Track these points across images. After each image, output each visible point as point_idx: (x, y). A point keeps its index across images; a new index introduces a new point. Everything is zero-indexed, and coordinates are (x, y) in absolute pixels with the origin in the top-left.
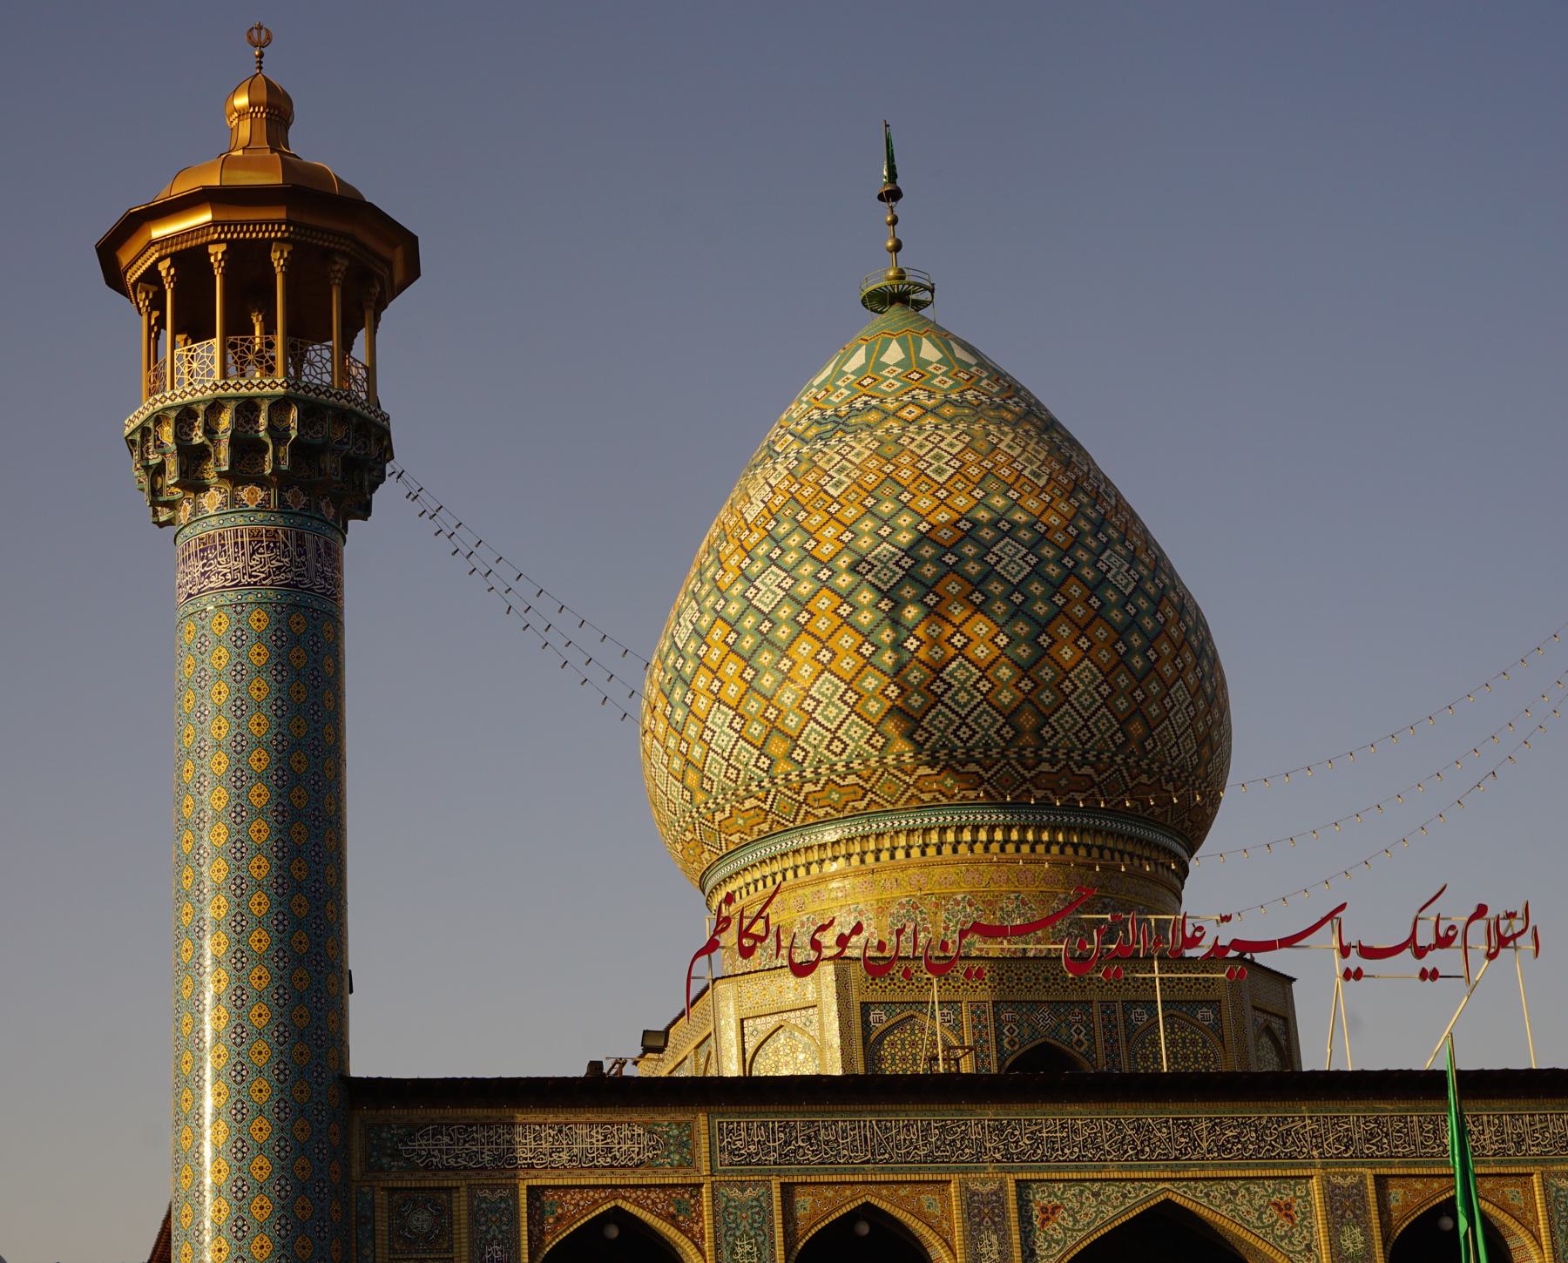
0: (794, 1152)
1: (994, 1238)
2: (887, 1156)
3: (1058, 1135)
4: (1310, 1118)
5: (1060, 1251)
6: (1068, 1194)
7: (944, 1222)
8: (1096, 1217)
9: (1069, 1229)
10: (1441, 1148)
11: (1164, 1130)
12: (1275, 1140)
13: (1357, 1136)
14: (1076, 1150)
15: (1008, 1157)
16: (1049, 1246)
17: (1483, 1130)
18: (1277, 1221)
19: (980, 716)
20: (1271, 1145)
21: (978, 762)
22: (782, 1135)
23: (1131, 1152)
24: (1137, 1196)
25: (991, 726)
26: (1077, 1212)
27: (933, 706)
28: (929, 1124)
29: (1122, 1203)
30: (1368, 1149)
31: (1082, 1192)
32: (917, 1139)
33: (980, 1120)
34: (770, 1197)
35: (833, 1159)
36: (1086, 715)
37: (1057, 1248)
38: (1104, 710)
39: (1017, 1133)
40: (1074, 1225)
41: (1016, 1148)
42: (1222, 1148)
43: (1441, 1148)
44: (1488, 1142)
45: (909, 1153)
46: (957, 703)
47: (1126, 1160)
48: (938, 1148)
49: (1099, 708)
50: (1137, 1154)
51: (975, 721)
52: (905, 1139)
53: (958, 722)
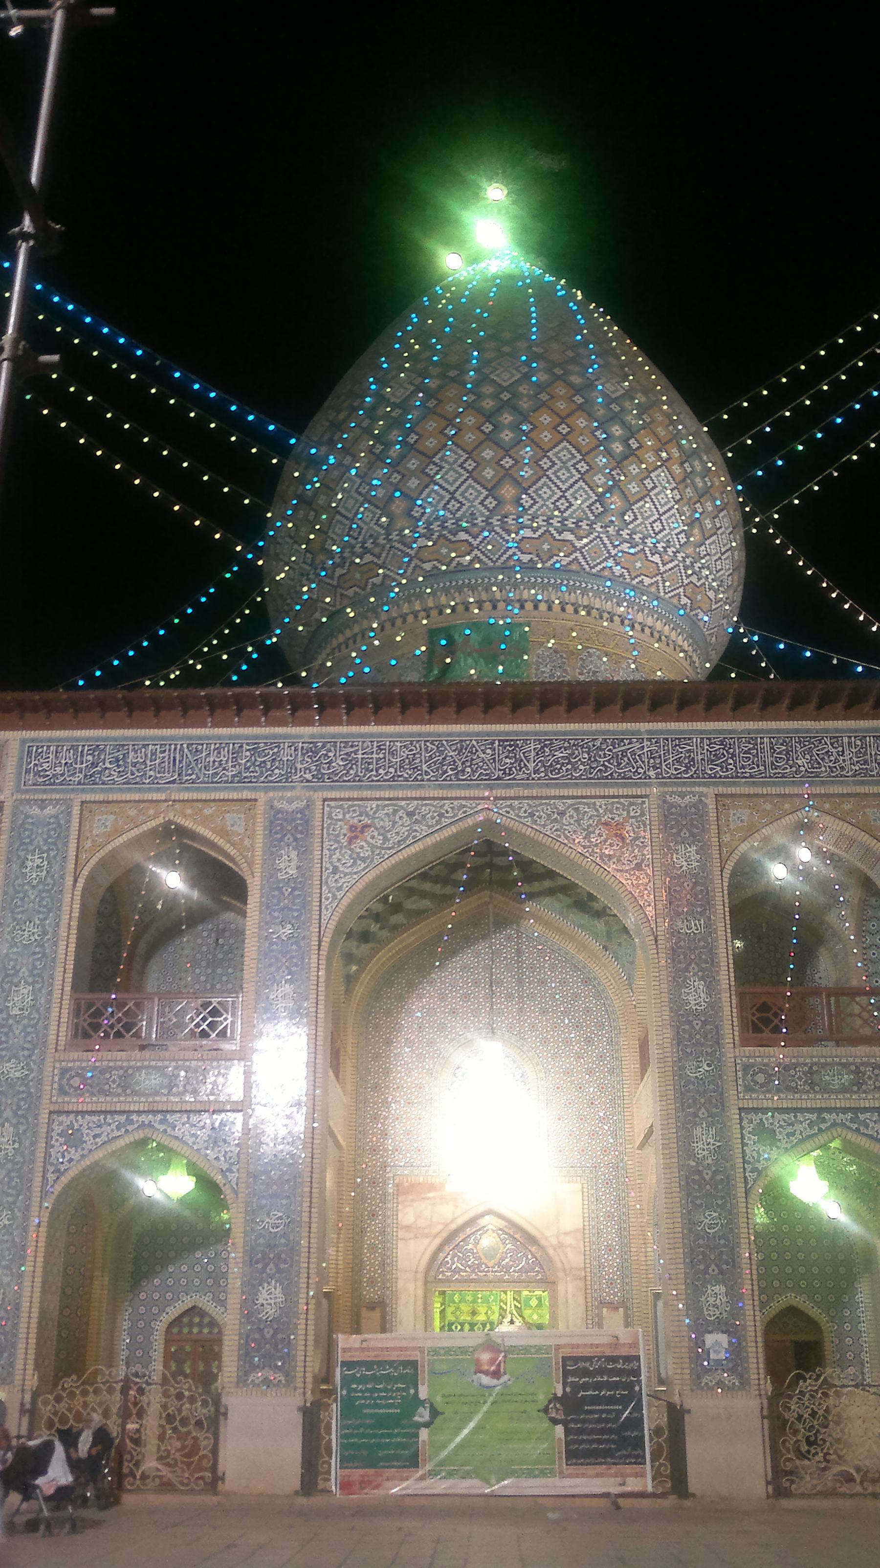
0: (100, 773)
1: (294, 854)
2: (194, 777)
3: (374, 756)
4: (650, 740)
5: (365, 868)
6: (381, 814)
7: (247, 840)
8: (408, 836)
9: (377, 847)
10: (794, 769)
11: (489, 751)
12: (608, 761)
13: (700, 757)
14: (392, 770)
15: (318, 776)
16: (354, 864)
17: (843, 752)
18: (605, 841)
19: (465, 491)
20: (603, 765)
21: (465, 530)
22: (90, 758)
23: (450, 773)
24: (457, 815)
25: (476, 498)
26: (389, 831)
27: (426, 486)
28: (241, 747)
29: (437, 823)
30: (711, 769)
31: (395, 811)
32: (227, 761)
33: (293, 743)
34: (69, 814)
35: (138, 779)
36: (564, 487)
37: (363, 866)
38: (581, 483)
39: (330, 754)
40: (384, 843)
41: (329, 768)
42: (551, 768)
43: (794, 769)
44: (848, 762)
45: (216, 774)
46: (446, 481)
47: (444, 780)
48: (247, 769)
49: (576, 482)
50: (457, 774)
51: (462, 494)
52: (214, 761)
53: (448, 496)
